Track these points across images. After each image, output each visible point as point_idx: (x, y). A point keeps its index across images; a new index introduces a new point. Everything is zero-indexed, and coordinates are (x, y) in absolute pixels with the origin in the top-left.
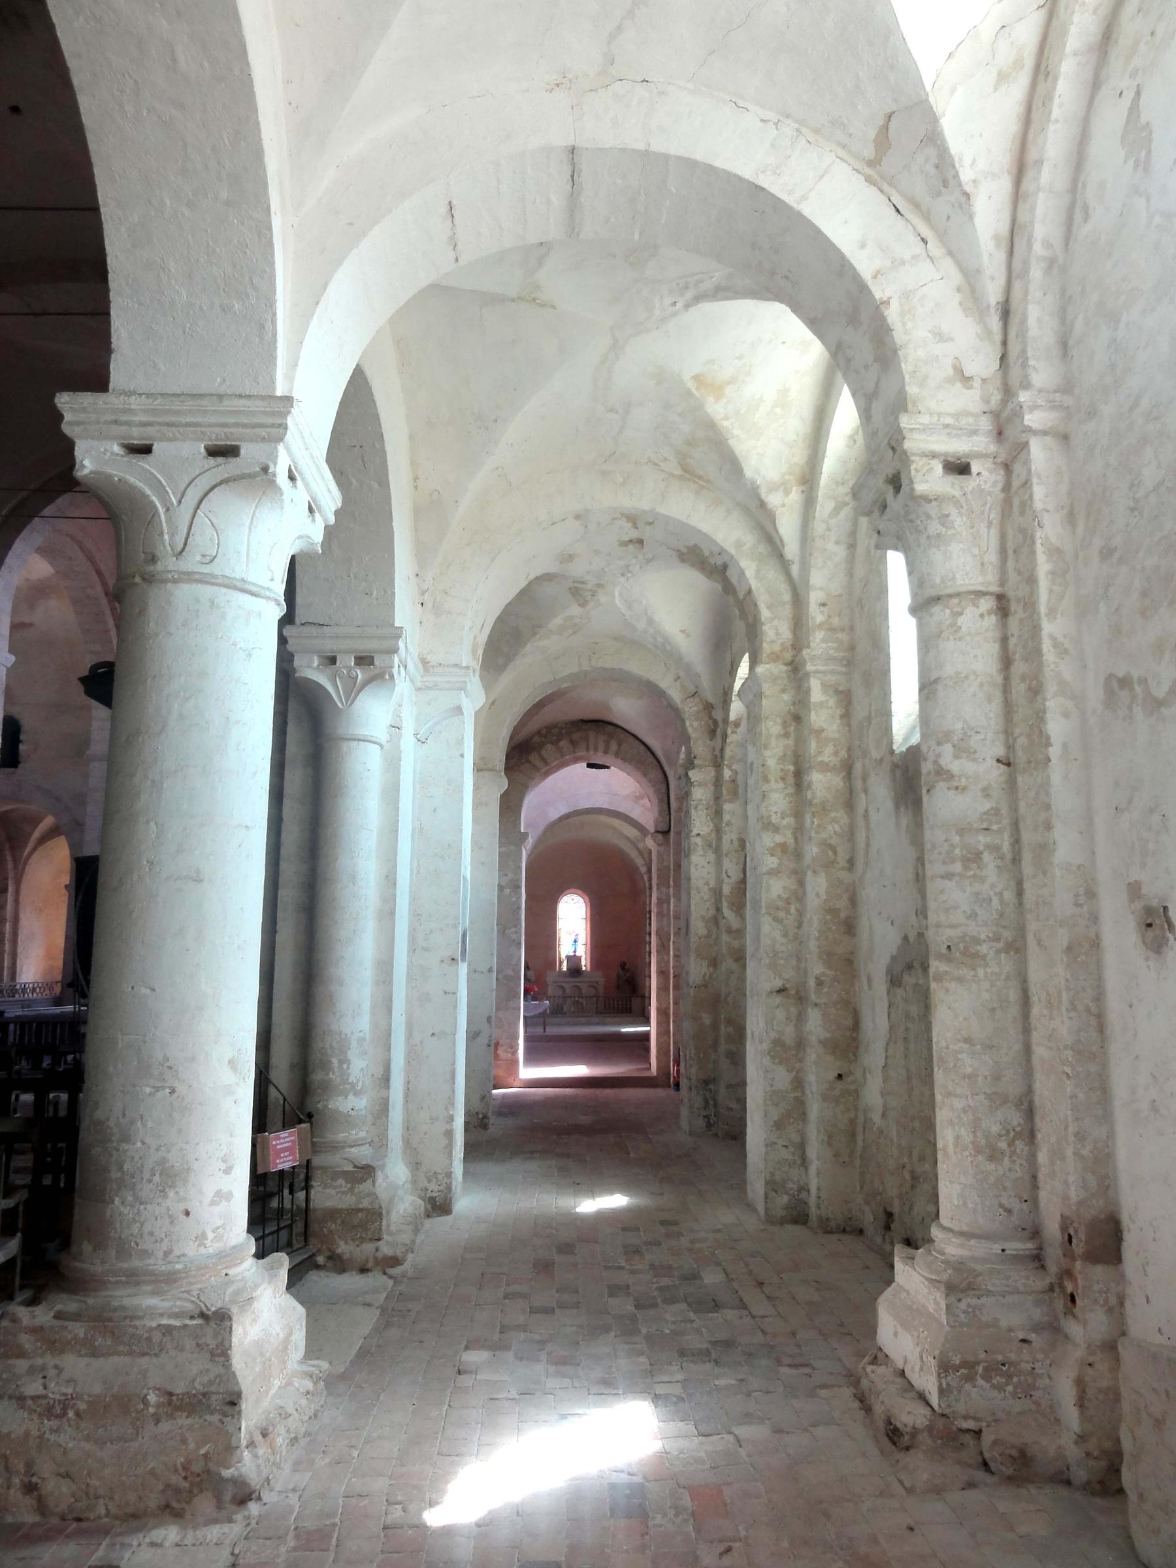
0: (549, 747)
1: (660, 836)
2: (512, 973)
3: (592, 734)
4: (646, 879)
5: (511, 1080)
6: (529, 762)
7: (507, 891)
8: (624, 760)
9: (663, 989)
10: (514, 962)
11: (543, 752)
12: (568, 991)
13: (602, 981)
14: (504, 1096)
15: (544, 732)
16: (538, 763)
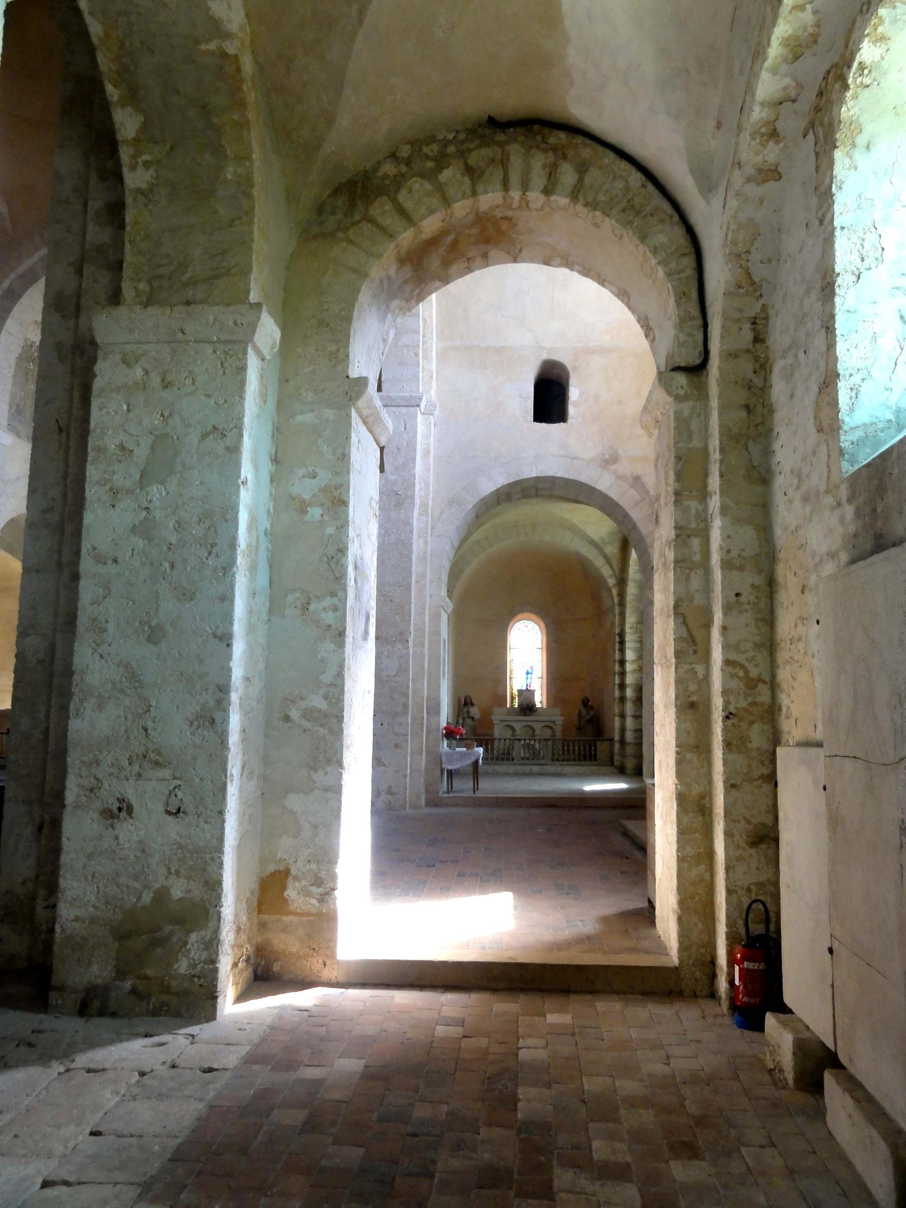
0: (417, 184)
1: (681, 379)
2: (322, 704)
3: (516, 152)
4: (615, 592)
5: (315, 965)
6: (371, 221)
7: (315, 512)
8: (593, 205)
9: (693, 748)
10: (326, 678)
11: (402, 196)
12: (518, 732)
13: (559, 720)
14: (278, 1027)
15: (405, 151)
16: (390, 220)
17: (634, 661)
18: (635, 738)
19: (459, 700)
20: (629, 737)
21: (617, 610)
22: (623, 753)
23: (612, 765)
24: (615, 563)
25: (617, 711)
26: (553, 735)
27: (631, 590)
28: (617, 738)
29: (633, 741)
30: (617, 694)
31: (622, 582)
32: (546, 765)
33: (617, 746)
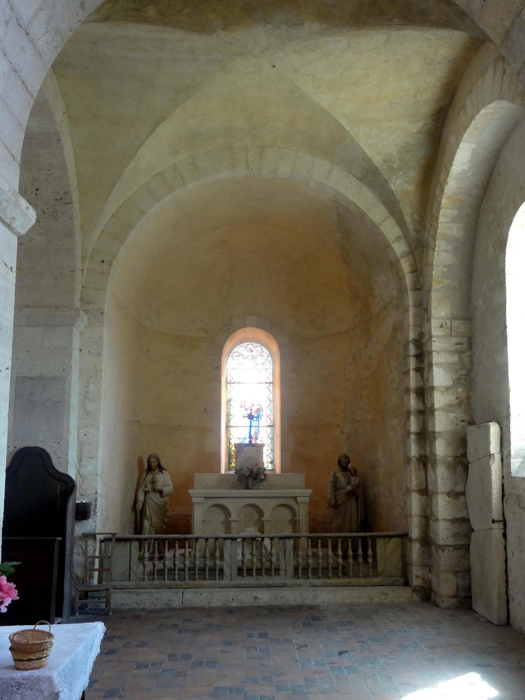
4: (405, 266)
13: (304, 495)
17: (448, 388)
18: (456, 535)
19: (140, 461)
20: (443, 532)
21: (410, 298)
22: (428, 565)
23: (407, 583)
24: (408, 211)
25: (414, 483)
26: (294, 522)
27: (442, 258)
28: (415, 533)
29: (451, 541)
30: (414, 451)
31: (420, 247)
32: (284, 586)
33: (416, 549)
